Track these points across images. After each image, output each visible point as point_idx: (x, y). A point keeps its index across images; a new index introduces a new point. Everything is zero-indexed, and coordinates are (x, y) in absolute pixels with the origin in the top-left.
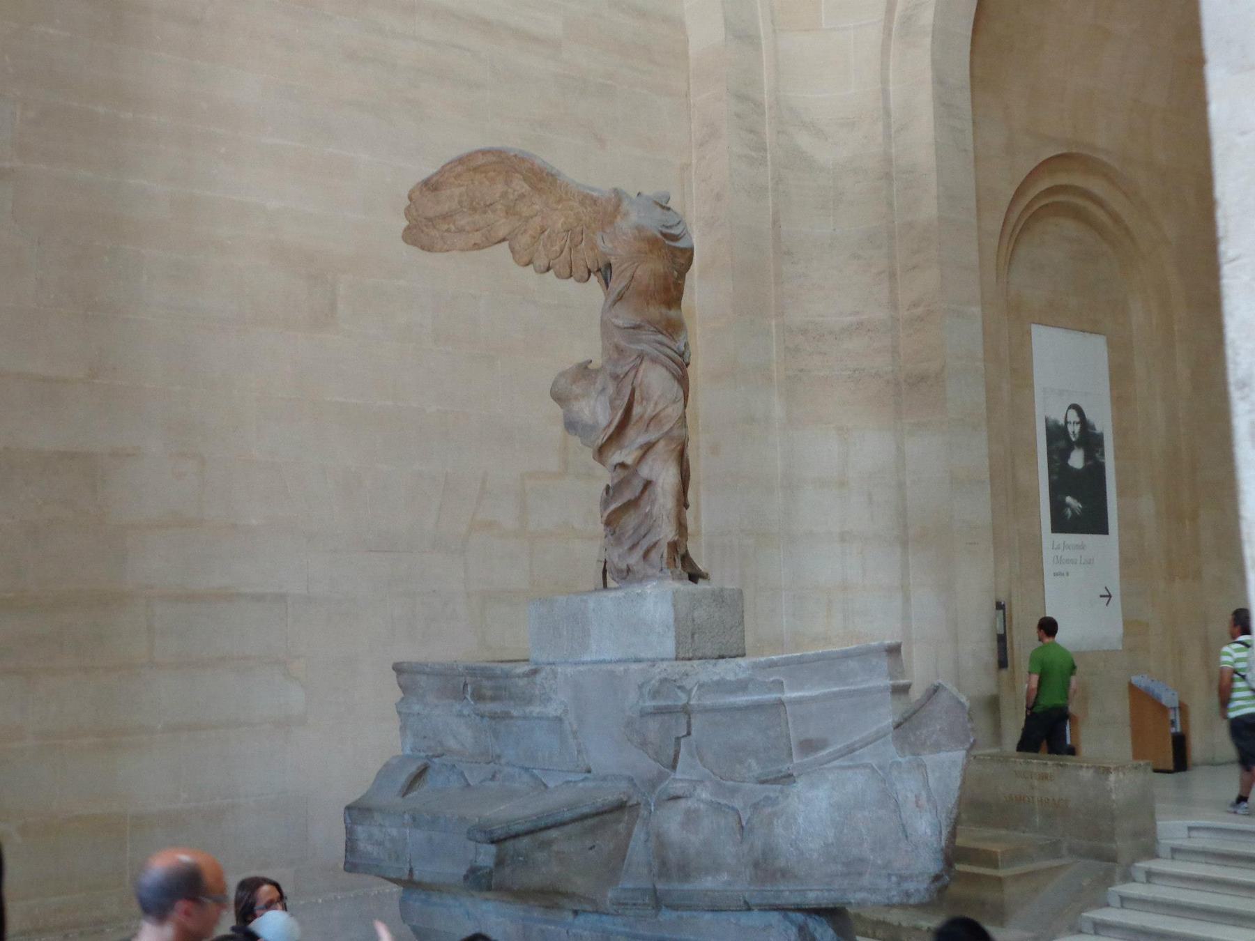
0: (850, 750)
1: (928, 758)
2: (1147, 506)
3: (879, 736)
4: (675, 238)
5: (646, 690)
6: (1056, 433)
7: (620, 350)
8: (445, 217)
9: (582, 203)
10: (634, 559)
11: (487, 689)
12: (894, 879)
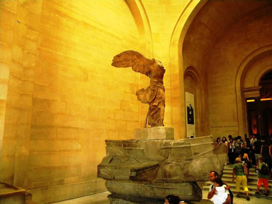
0: (204, 154)
1: (219, 155)
2: (199, 121)
3: (209, 152)
5: (162, 144)
6: (188, 108)
7: (154, 85)
8: (120, 61)
9: (147, 61)
10: (156, 122)
11: (127, 145)
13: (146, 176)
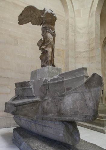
0: (76, 89)
1: (92, 89)
4: (54, 15)
8: (23, 19)
9: (40, 12)
12: (84, 116)
13: (26, 112)
